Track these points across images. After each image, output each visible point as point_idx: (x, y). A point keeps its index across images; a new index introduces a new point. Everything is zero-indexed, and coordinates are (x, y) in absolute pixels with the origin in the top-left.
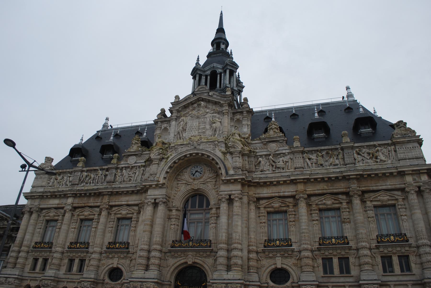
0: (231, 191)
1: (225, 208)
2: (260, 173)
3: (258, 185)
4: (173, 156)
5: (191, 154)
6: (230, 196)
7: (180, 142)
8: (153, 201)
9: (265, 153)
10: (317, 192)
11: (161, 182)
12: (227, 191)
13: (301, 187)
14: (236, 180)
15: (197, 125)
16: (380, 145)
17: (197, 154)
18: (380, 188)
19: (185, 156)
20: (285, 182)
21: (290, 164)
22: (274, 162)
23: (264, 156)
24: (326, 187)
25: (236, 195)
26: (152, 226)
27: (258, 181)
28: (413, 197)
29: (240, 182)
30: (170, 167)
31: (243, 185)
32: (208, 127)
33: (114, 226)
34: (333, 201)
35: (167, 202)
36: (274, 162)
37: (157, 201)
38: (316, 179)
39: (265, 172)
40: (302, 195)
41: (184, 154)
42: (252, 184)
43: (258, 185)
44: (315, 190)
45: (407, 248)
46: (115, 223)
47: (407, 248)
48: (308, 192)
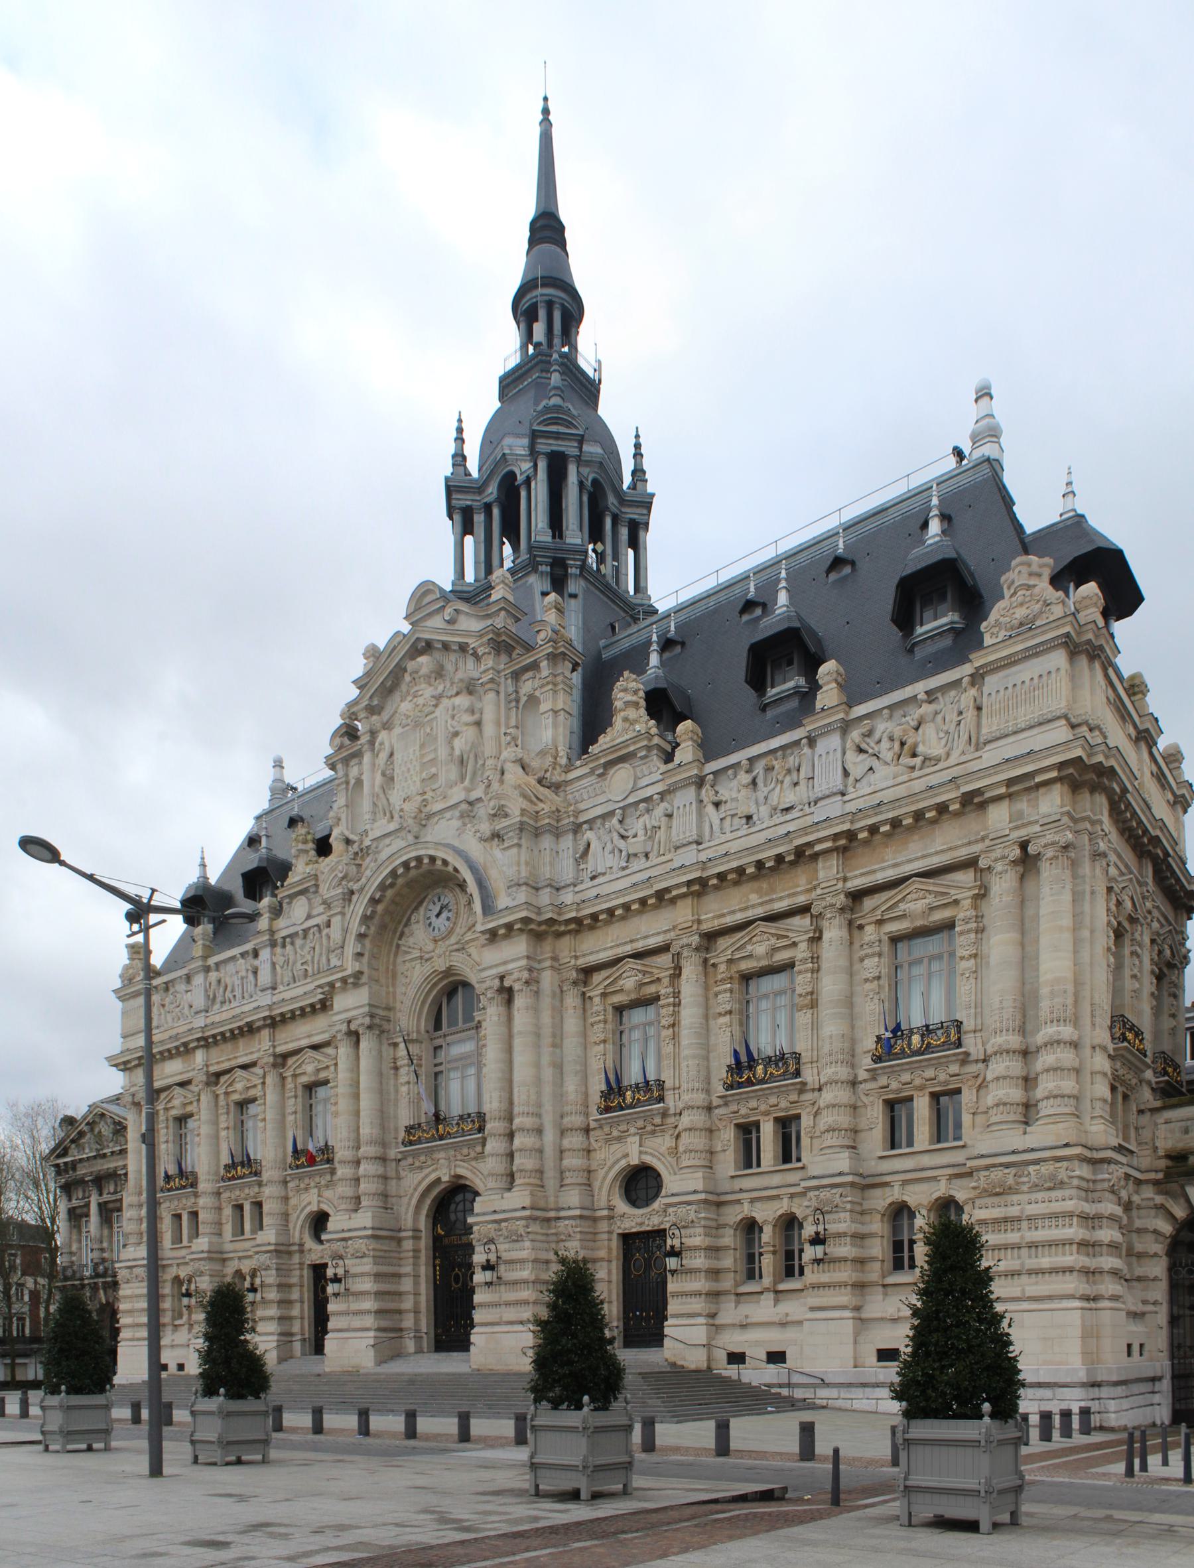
0: (505, 963)
1: (495, 1018)
2: (590, 884)
3: (581, 925)
4: (373, 877)
5: (406, 865)
6: (502, 978)
7: (383, 826)
8: (344, 1027)
9: (599, 811)
10: (729, 920)
11: (349, 972)
12: (496, 966)
13: (683, 913)
14: (509, 927)
15: (418, 753)
16: (931, 696)
17: (419, 859)
18: (907, 869)
19: (393, 873)
20: (643, 901)
21: (661, 834)
22: (623, 837)
23: (599, 821)
24: (754, 898)
25: (515, 976)
26: (356, 1096)
27: (573, 914)
28: (1003, 885)
29: (520, 930)
30: (366, 919)
31: (538, 937)
32: (443, 753)
33: (300, 1108)
34: (773, 941)
35: (380, 1022)
36: (623, 837)
37: (353, 1027)
38: (721, 876)
39: (610, 875)
40: (685, 941)
41: (390, 869)
42: (563, 928)
43: (581, 925)
44: (723, 915)
45: (954, 1068)
46: (300, 1100)
47: (954, 1068)
48: (706, 927)
